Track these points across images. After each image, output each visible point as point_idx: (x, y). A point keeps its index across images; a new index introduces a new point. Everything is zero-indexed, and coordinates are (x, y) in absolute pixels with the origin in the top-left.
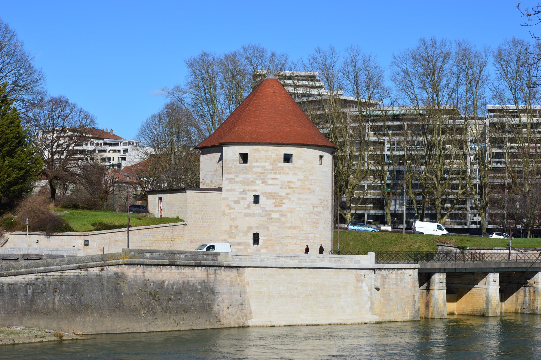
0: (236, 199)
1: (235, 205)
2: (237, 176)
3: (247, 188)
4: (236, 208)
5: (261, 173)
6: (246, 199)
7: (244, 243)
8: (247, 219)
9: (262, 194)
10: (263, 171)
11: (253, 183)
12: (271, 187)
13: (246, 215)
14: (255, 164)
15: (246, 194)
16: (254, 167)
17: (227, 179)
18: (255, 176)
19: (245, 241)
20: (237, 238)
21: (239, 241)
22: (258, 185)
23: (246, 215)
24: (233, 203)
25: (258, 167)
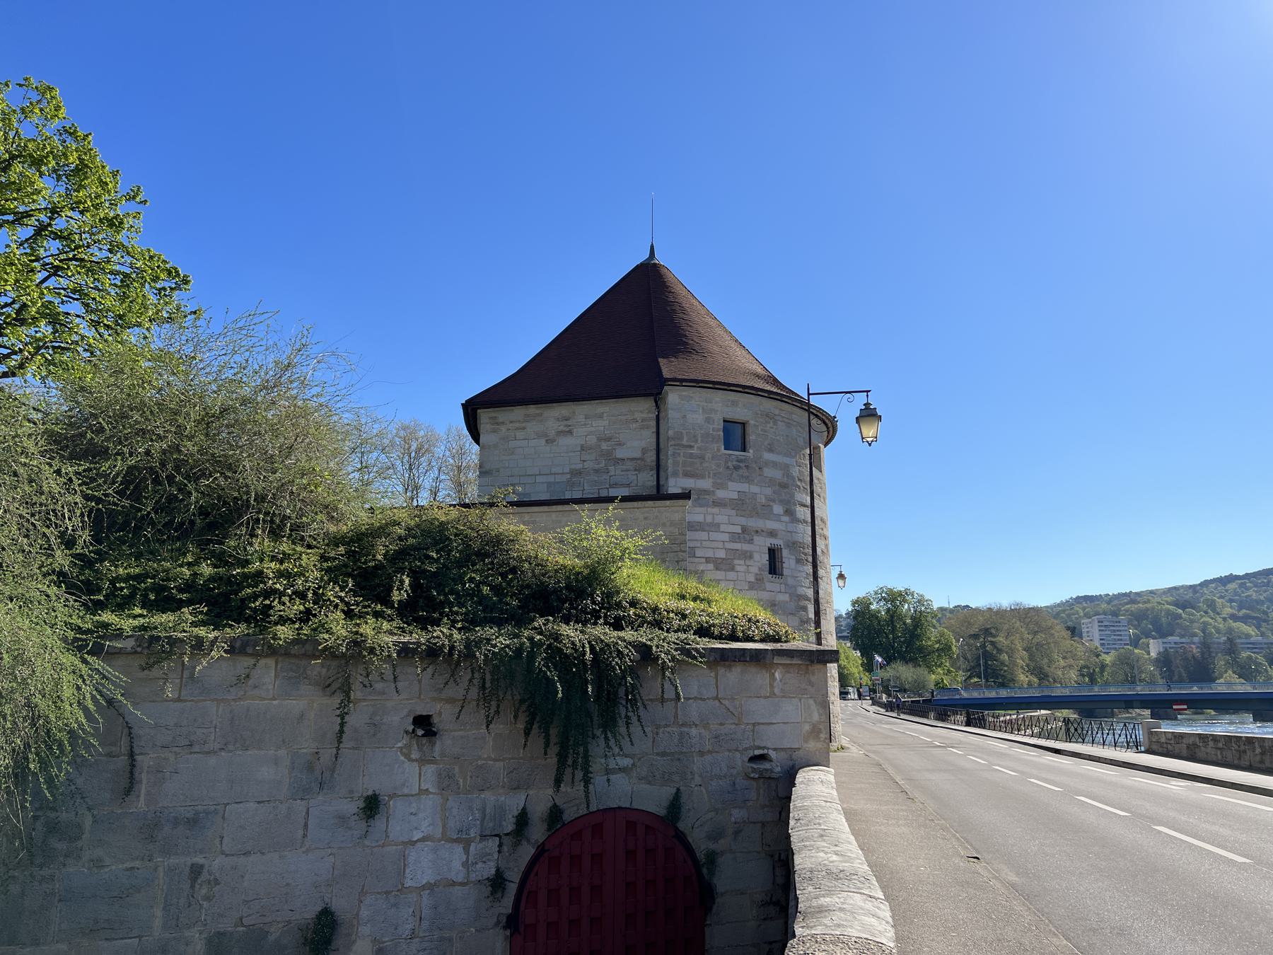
0: (721, 554)
3: (754, 523)
6: (751, 557)
14: (768, 456)
15: (751, 541)
16: (767, 463)
18: (768, 491)
22: (777, 518)
24: (711, 566)
25: (775, 465)
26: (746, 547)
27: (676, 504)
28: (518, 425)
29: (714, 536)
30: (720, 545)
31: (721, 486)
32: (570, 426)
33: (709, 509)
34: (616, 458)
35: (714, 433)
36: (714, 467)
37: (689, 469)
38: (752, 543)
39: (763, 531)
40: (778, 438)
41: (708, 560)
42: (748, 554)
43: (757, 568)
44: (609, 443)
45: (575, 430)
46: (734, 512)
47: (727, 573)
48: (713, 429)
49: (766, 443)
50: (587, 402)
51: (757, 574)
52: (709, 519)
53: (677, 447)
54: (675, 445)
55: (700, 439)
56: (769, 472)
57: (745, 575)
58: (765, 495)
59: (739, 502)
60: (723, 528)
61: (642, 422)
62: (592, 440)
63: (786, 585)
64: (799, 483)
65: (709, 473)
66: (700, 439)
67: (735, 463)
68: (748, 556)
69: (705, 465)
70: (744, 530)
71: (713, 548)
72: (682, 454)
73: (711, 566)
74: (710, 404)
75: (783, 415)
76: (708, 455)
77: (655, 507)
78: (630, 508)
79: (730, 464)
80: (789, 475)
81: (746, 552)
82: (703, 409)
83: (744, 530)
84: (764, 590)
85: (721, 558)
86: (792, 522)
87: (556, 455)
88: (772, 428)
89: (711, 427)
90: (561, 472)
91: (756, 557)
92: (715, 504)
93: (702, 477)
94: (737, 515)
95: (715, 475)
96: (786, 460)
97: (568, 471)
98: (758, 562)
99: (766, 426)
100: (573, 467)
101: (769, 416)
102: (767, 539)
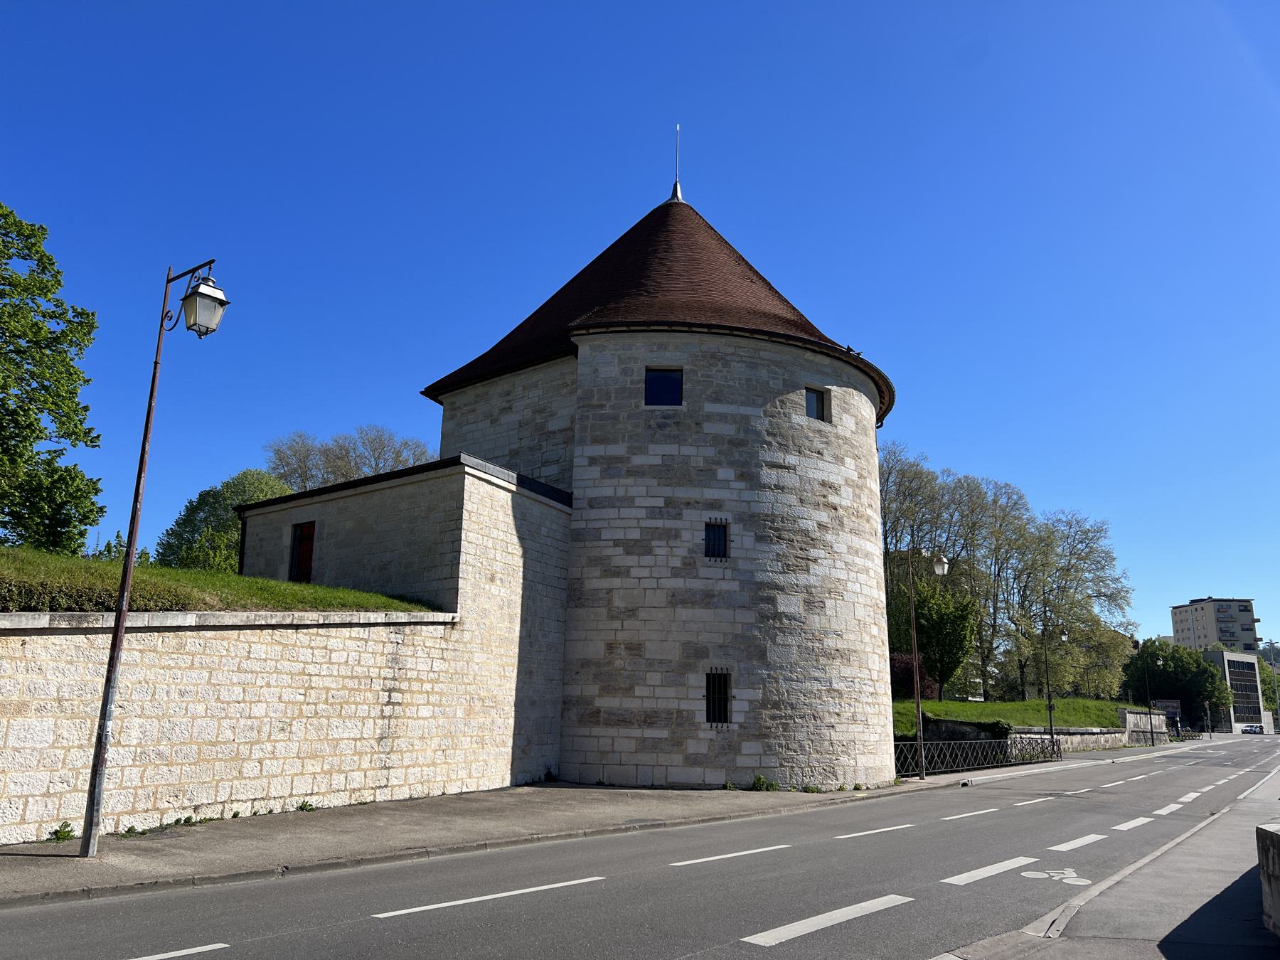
0: (635, 535)
1: (630, 561)
2: (634, 451)
3: (683, 493)
4: (634, 572)
5: (731, 442)
7: (669, 713)
8: (684, 613)
9: (740, 519)
10: (741, 436)
12: (604, 542)
13: (676, 600)
14: (710, 407)
15: (678, 516)
16: (709, 417)
17: (593, 461)
18: (710, 452)
19: (673, 705)
20: (639, 691)
21: (649, 705)
22: (725, 484)
23: (676, 600)
24: (620, 550)
25: (723, 418)
26: (669, 524)
27: (454, 472)
28: (469, 408)
29: (625, 512)
30: (634, 523)
31: (642, 451)
32: (510, 401)
33: (621, 480)
34: (548, 432)
35: (632, 386)
36: (630, 428)
37: (598, 433)
38: (680, 519)
39: (698, 503)
40: (731, 383)
41: (617, 543)
42: (673, 532)
43: (686, 550)
44: (543, 415)
45: (515, 404)
46: (655, 482)
47: (641, 557)
48: (632, 383)
49: (709, 392)
50: (524, 371)
51: (685, 557)
52: (621, 492)
53: (585, 409)
54: (583, 407)
55: (613, 395)
56: (710, 428)
57: (667, 560)
58: (704, 457)
59: (664, 469)
60: (638, 502)
61: (572, 385)
62: (528, 413)
63: (734, 570)
64: (769, 439)
65: (624, 436)
66: (613, 395)
67: (659, 420)
69: (619, 426)
70: (669, 502)
71: (625, 528)
72: (591, 417)
73: (620, 550)
74: (629, 352)
75: (742, 354)
76: (623, 415)
77: (439, 477)
78: (418, 482)
79: (652, 422)
80: (749, 430)
81: (670, 530)
82: (619, 358)
83: (669, 502)
84: (696, 577)
85: (634, 540)
86: (752, 489)
87: (499, 435)
88: (722, 371)
89: (629, 379)
90: (502, 454)
91: (686, 535)
92: (631, 473)
93: (615, 441)
94: (659, 485)
95: (631, 437)
96: (745, 410)
97: (506, 453)
98: (688, 541)
99: (711, 371)
100: (513, 447)
101: (714, 357)
102: (704, 512)
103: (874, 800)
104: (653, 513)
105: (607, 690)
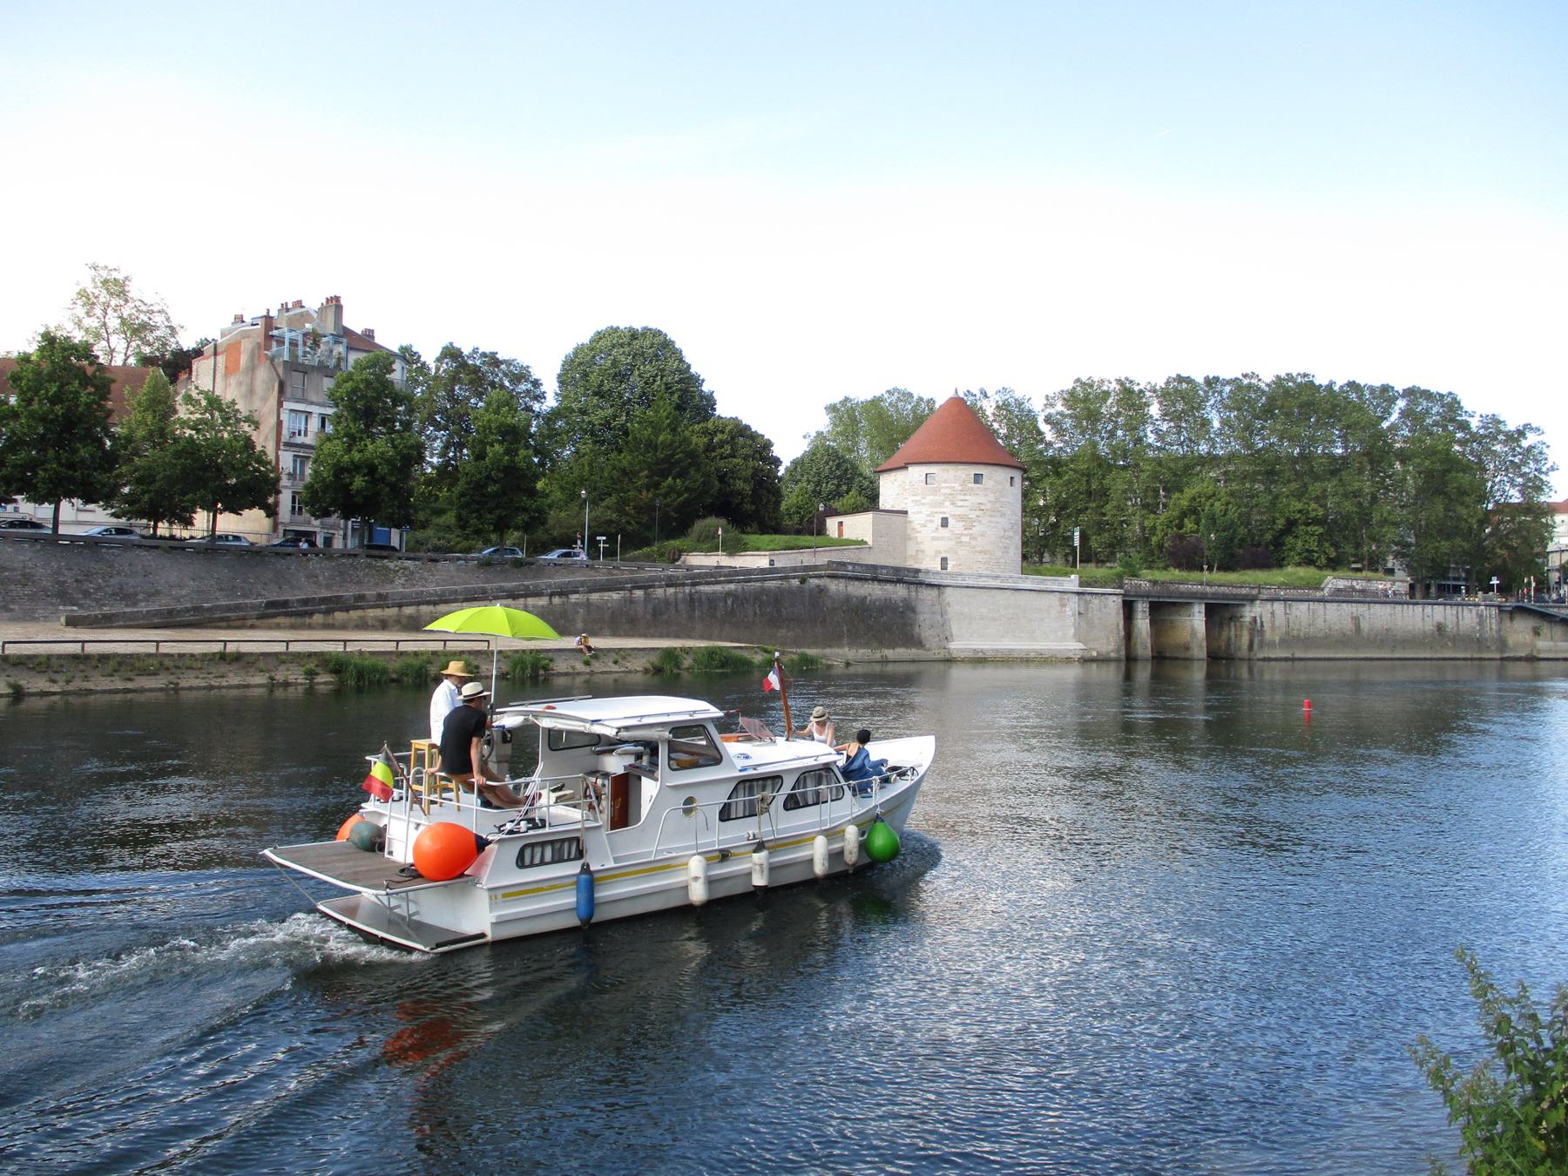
3: (935, 510)
8: (935, 542)
9: (951, 515)
11: (941, 504)
13: (934, 538)
14: (943, 485)
23: (934, 538)
56: (943, 491)
68: (932, 521)
103: (1310, 656)
104: (928, 516)
105: (916, 563)
